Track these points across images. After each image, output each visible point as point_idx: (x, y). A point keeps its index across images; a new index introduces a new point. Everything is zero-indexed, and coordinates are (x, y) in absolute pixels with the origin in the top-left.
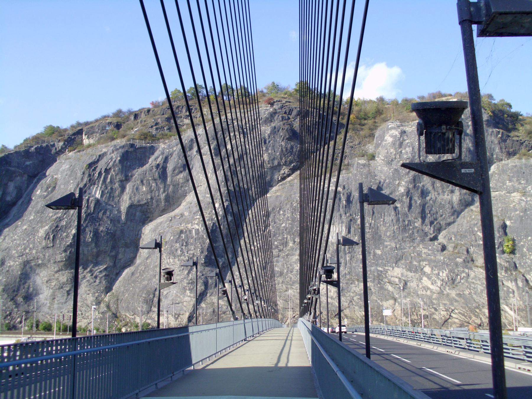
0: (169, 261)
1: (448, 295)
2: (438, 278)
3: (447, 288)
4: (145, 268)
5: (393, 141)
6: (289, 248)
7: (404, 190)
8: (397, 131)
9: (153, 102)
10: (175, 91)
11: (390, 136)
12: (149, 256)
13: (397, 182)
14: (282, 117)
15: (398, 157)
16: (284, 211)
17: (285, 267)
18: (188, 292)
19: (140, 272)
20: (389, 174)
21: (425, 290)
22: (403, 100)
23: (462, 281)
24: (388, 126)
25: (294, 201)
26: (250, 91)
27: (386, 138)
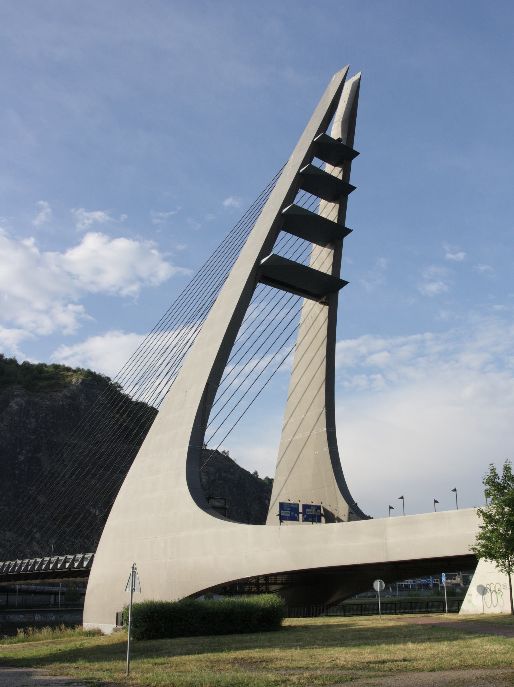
5: (18, 408)
7: (24, 458)
8: (23, 399)
11: (15, 403)
13: (18, 450)
15: (22, 426)
27: (10, 404)
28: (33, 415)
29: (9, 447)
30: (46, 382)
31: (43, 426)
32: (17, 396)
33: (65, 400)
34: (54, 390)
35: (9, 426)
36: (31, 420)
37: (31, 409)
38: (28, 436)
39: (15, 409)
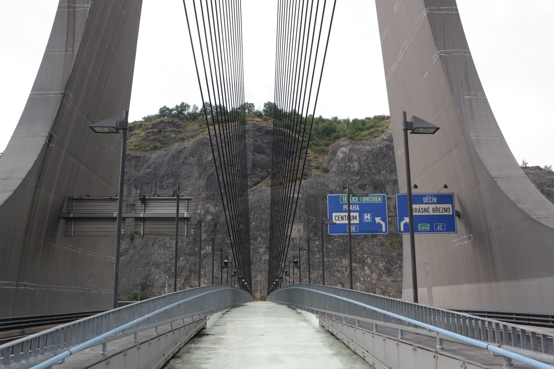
0: (160, 252)
1: (384, 281)
2: (377, 268)
3: (384, 276)
4: (139, 257)
5: (343, 156)
8: (347, 148)
9: (145, 117)
11: (341, 152)
12: (142, 247)
14: (254, 135)
15: (347, 170)
16: (255, 212)
17: (255, 257)
19: (135, 261)
20: (340, 183)
21: (366, 277)
22: (353, 121)
23: (396, 271)
24: (340, 144)
25: (262, 204)
27: (337, 154)
28: (356, 159)
29: (338, 189)
30: (368, 131)
31: (365, 167)
32: (343, 146)
33: (382, 142)
34: (374, 136)
35: (337, 172)
36: (354, 163)
37: (354, 155)
38: (353, 177)
39: (341, 157)
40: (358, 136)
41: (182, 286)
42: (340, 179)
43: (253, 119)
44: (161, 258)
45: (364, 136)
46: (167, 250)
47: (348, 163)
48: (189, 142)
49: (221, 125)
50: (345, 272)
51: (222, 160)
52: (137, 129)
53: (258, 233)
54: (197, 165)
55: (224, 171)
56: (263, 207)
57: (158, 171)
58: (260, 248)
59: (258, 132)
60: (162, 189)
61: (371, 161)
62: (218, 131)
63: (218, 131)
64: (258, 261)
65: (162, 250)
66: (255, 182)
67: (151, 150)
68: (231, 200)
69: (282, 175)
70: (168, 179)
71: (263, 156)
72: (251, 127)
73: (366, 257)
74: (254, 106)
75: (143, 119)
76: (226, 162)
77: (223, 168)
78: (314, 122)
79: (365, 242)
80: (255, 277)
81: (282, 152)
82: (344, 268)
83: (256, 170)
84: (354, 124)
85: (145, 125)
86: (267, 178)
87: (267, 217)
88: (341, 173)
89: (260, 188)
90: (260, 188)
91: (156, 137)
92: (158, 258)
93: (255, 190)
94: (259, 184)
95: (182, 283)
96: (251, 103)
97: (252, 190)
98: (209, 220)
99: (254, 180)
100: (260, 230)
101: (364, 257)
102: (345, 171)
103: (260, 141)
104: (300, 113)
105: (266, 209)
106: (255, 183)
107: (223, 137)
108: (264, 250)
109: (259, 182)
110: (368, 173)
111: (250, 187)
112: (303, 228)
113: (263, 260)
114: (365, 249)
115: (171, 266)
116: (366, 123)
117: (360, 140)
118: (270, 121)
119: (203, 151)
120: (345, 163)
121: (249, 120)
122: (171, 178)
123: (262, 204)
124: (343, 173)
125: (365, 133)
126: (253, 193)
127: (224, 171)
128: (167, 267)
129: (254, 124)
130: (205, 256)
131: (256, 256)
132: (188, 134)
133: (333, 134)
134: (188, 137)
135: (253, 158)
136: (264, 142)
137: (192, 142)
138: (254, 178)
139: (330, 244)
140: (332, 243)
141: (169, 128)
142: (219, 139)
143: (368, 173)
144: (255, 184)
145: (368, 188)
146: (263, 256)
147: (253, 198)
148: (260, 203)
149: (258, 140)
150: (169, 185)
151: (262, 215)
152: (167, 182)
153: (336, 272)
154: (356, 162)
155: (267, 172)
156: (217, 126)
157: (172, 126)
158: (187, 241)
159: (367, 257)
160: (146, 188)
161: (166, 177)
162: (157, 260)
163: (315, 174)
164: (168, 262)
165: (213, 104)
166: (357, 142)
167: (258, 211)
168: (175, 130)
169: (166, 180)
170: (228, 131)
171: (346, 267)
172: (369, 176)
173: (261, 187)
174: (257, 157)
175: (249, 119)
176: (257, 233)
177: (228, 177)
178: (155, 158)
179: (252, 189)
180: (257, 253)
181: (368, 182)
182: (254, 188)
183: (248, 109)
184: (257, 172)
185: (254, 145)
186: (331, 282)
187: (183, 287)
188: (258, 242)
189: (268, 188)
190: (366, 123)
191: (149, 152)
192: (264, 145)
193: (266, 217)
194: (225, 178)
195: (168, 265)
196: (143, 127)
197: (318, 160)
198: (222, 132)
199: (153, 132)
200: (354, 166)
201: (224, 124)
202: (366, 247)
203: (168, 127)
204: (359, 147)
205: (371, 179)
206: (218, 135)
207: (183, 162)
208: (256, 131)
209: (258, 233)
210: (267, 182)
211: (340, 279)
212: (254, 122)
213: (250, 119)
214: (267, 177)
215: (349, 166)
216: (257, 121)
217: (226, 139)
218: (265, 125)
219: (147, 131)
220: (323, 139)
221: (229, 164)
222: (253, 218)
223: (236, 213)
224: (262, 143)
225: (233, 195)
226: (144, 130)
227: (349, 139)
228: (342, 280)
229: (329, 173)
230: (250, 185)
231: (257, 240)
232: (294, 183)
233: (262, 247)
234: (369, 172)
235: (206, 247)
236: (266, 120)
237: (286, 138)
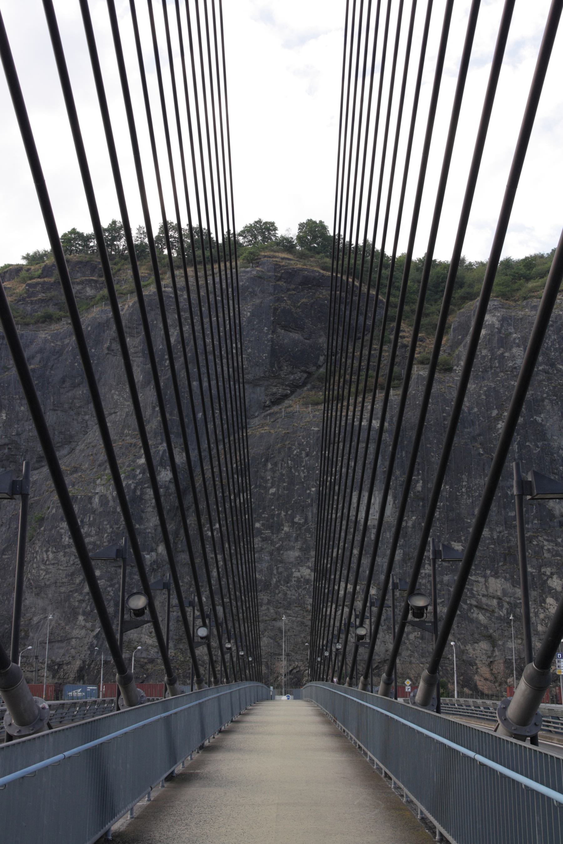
0: (45, 556)
6: (282, 535)
8: (494, 316)
9: (28, 255)
10: (70, 233)
13: (495, 413)
14: (275, 287)
15: (497, 365)
16: (275, 464)
17: (275, 572)
18: (81, 618)
20: (479, 396)
25: (294, 445)
26: (213, 235)
28: (517, 341)
29: (476, 410)
36: (514, 350)
40: (518, 290)
41: (95, 642)
42: (481, 387)
43: (272, 253)
44: (47, 573)
45: (532, 290)
46: (62, 553)
47: (499, 349)
48: (124, 305)
49: (200, 267)
50: (497, 610)
51: (200, 342)
52: (9, 280)
53: (283, 513)
54: (141, 354)
55: (203, 370)
56: (295, 452)
57: (51, 369)
58: (287, 550)
59: (285, 282)
60: (59, 412)
61: (553, 344)
62: (192, 280)
63: (192, 280)
64: (282, 582)
65: (49, 553)
66: (278, 396)
67: (36, 323)
68: (220, 437)
69: (342, 380)
70: (74, 387)
71: (296, 336)
72: (269, 271)
73: (548, 573)
74: (275, 229)
75: (24, 258)
76: (209, 348)
77: (202, 362)
78: (412, 270)
79: (545, 537)
80: (275, 620)
81: (341, 328)
82: (495, 602)
83: (280, 368)
84: (506, 269)
85: (28, 270)
86: (305, 386)
87: (305, 476)
88: (482, 372)
89: (289, 410)
90: (289, 410)
91: (49, 295)
92: (41, 572)
93: (277, 413)
94: (286, 402)
95: (95, 633)
96: (269, 220)
97: (270, 414)
98: (166, 481)
99: (274, 390)
100: (288, 506)
101: (544, 574)
102: (491, 368)
103: (289, 302)
104: (378, 246)
105: (304, 454)
106: (278, 399)
107: (203, 293)
108: (297, 554)
109: (286, 397)
110: (547, 372)
111: (265, 407)
112: (391, 503)
113: (296, 579)
114: (546, 555)
115: (71, 591)
116: (535, 265)
117: (525, 298)
118: (312, 259)
119: (155, 322)
120: (491, 350)
121: (265, 256)
122: (79, 385)
123: (294, 445)
124: (487, 371)
125: (535, 284)
126: (272, 420)
127: (203, 370)
128: (61, 593)
129: (277, 265)
130: (155, 567)
131: (277, 569)
132: (123, 287)
133: (459, 291)
134: (122, 294)
135: (272, 340)
136: (299, 304)
137: (131, 304)
138: (276, 386)
139: (458, 542)
140: (463, 538)
141: (81, 277)
142: (194, 296)
143: (547, 372)
144: (277, 401)
145: (548, 408)
146: (294, 570)
147: (272, 431)
148: (287, 442)
149: (285, 298)
150: (76, 401)
151: (293, 470)
152: (70, 394)
153: (475, 609)
154: (518, 346)
155: (305, 372)
156: (190, 271)
157: (88, 272)
158: (112, 532)
159: (552, 574)
160: (22, 408)
161: (67, 384)
162: (39, 576)
163: (419, 375)
164: (63, 583)
165: (184, 225)
166: (519, 303)
167: (283, 461)
168: (96, 282)
169: (68, 392)
170: (217, 279)
171: (500, 599)
172: (549, 379)
173: (290, 406)
174: (281, 337)
175: (263, 254)
176: (279, 514)
177: (213, 383)
178: (46, 341)
179: (269, 412)
180: (281, 562)
181: (547, 393)
182: (275, 409)
183: (263, 234)
184: (282, 373)
185: (275, 309)
186: (462, 636)
187: (98, 642)
188: (283, 535)
189: (306, 408)
190: (535, 265)
191: (31, 327)
192: (299, 310)
193: (302, 475)
194: (205, 384)
195: (63, 589)
196: (23, 274)
197: (424, 344)
198: (202, 282)
199: (44, 283)
200: (514, 356)
201: (209, 267)
202: (548, 550)
203: (79, 275)
204: (523, 313)
205: (554, 387)
206: (193, 288)
207: (109, 348)
208: (280, 279)
209: (283, 513)
210: (303, 395)
211: (486, 627)
212: (274, 259)
213: (266, 254)
214: (305, 384)
215: (502, 356)
216: (283, 259)
217: (211, 296)
218: (300, 266)
219: (29, 282)
220: (436, 302)
221: (217, 353)
222: (272, 478)
223: (229, 466)
224: (294, 306)
225: (225, 426)
226: (24, 281)
227: (497, 297)
228: (491, 631)
229: (452, 374)
230: (265, 402)
231: (279, 530)
232: (369, 398)
233: (292, 548)
234: (550, 371)
235: (158, 546)
236: (302, 256)
237: (349, 296)
